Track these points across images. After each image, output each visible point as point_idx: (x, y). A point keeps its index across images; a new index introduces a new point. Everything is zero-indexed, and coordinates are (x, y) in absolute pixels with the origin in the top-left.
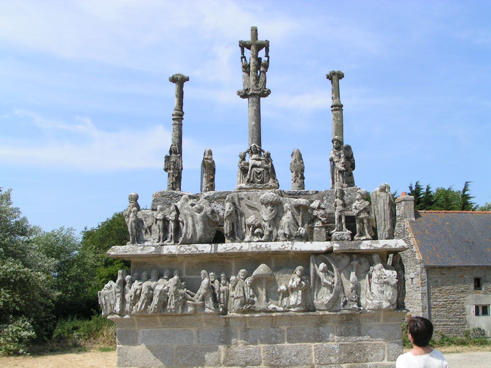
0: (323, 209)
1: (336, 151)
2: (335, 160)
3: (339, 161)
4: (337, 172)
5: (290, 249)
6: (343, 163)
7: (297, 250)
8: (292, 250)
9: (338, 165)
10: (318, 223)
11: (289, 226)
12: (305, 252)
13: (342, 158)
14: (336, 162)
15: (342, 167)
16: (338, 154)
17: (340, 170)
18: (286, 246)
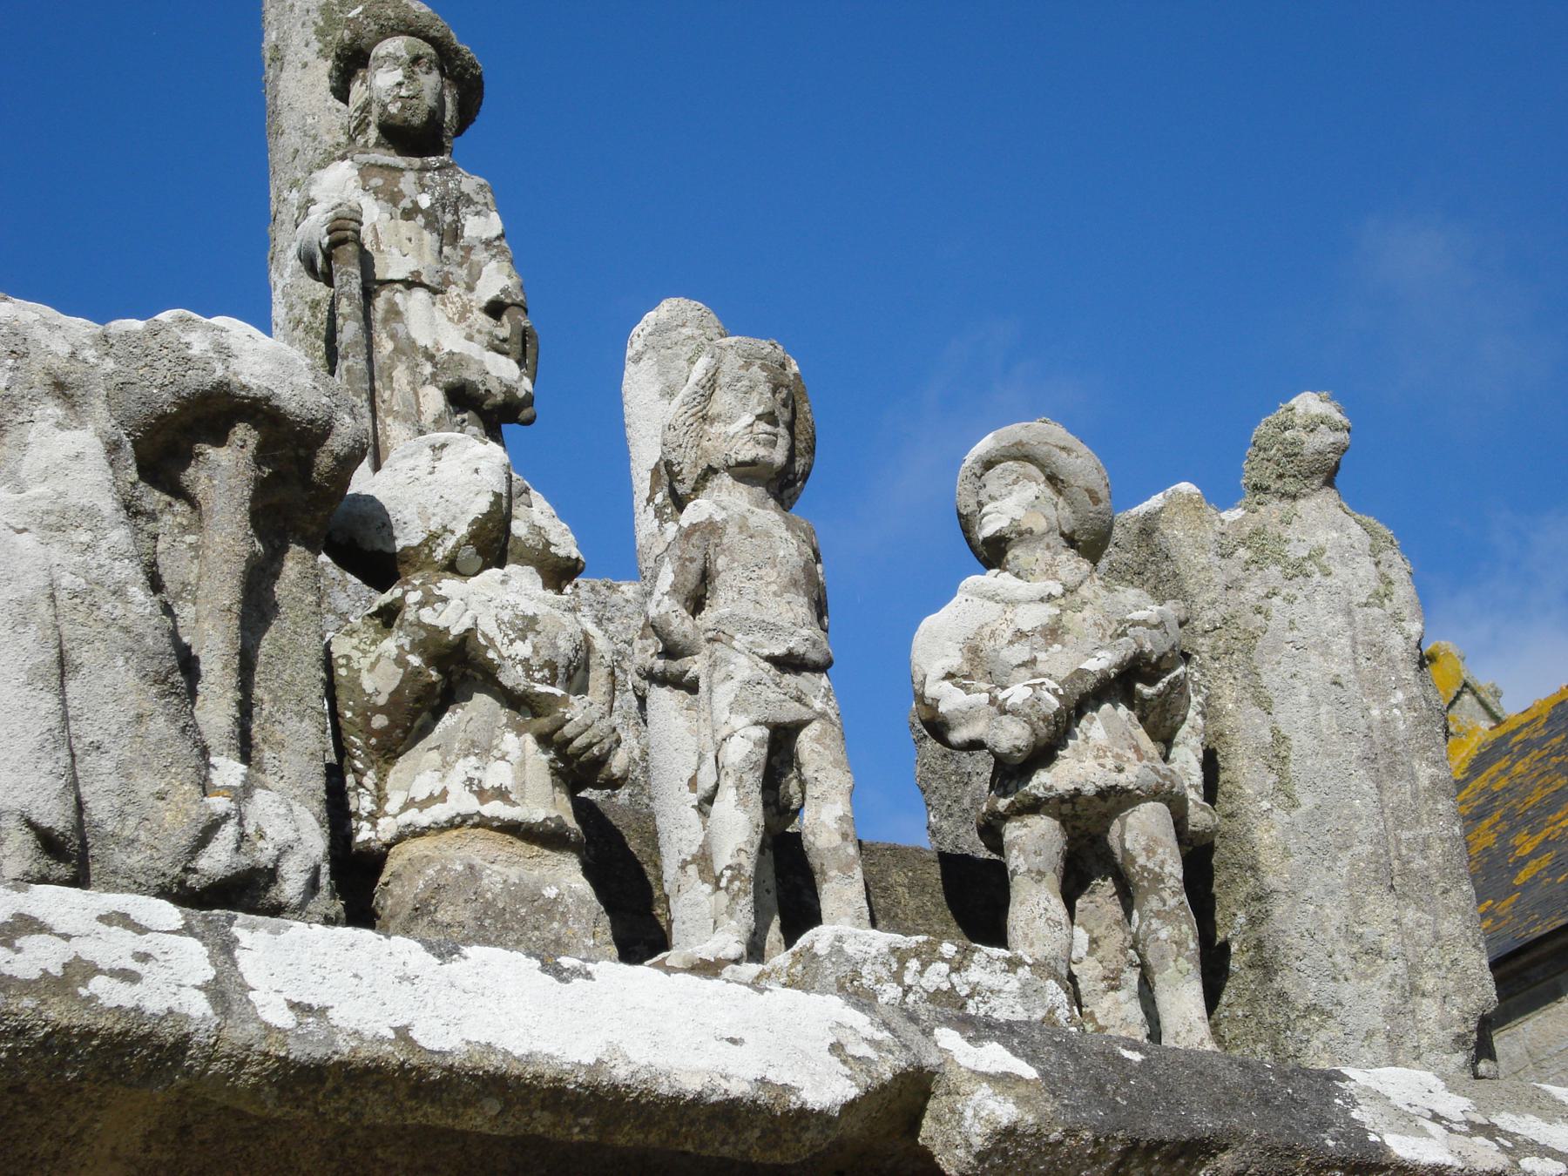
0: (559, 573)
1: (400, 161)
2: (393, 265)
3: (446, 281)
4: (433, 400)
5: (198, 1006)
6: (495, 309)
7: (763, 760)
8: (238, 1034)
9: (432, 322)
10: (498, 774)
11: (63, 666)
12: (481, 1119)
13: (480, 255)
14: (411, 284)
15: (498, 347)
16: (425, 201)
17: (472, 375)
18: (89, 950)
